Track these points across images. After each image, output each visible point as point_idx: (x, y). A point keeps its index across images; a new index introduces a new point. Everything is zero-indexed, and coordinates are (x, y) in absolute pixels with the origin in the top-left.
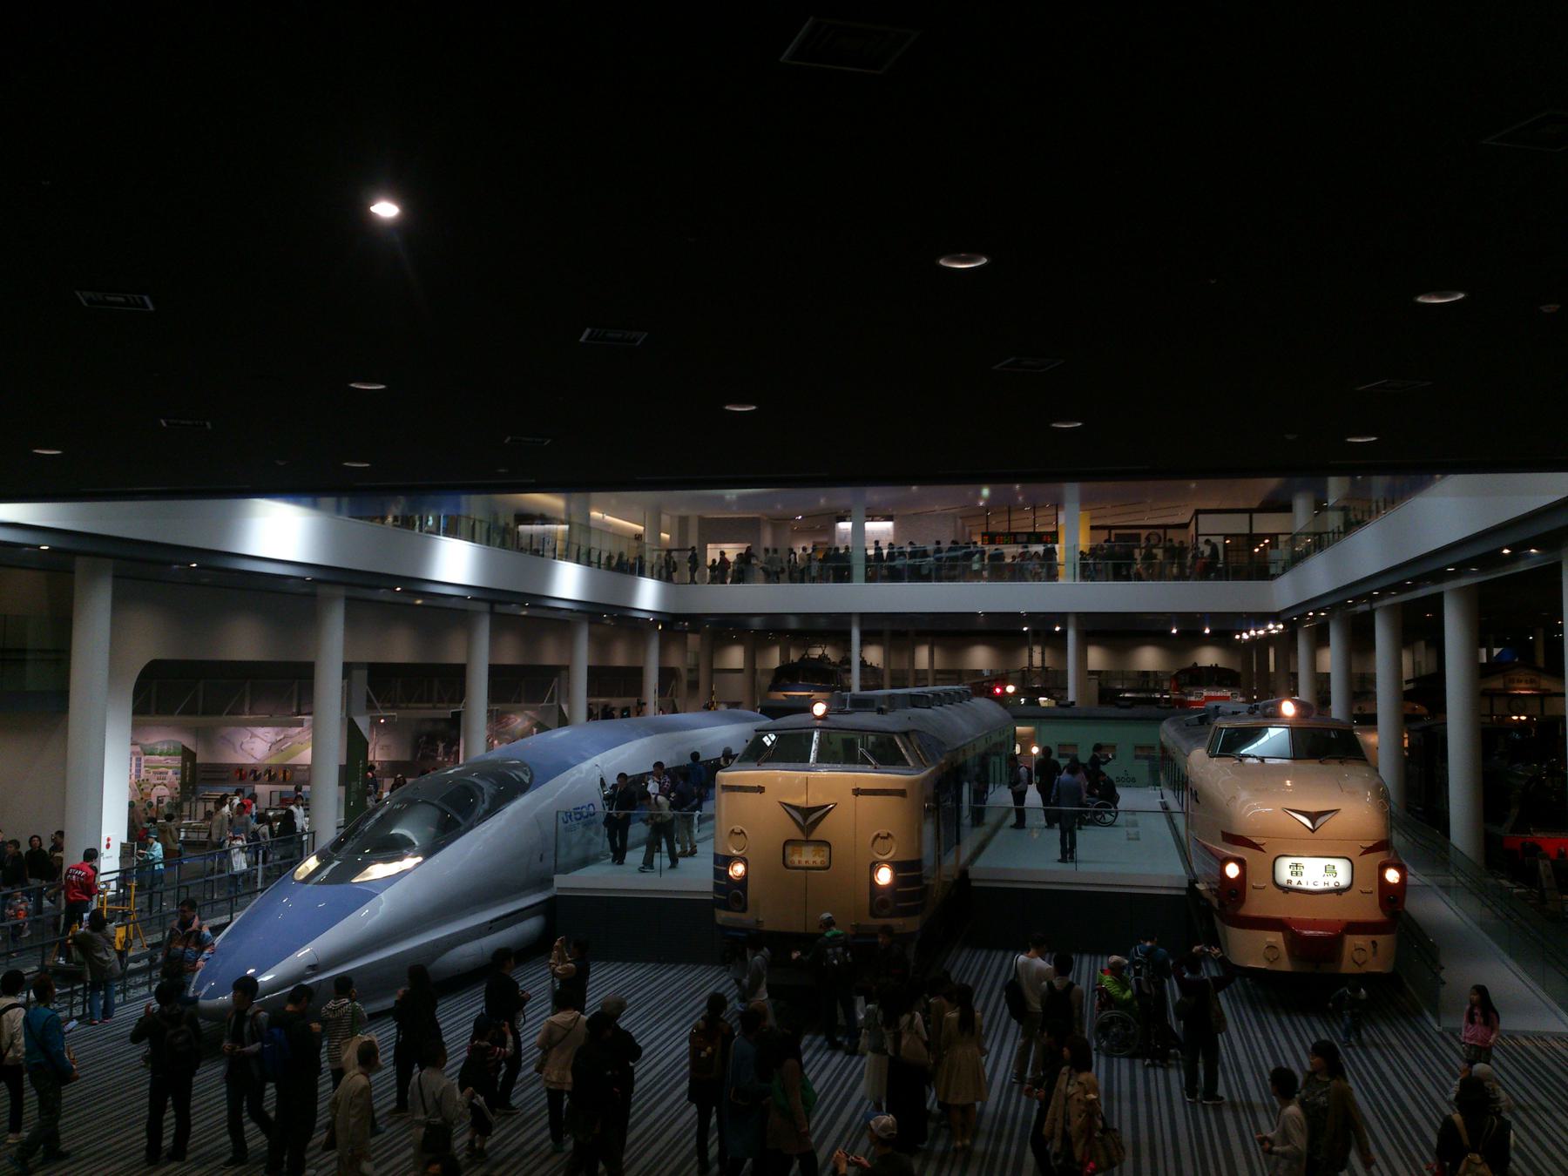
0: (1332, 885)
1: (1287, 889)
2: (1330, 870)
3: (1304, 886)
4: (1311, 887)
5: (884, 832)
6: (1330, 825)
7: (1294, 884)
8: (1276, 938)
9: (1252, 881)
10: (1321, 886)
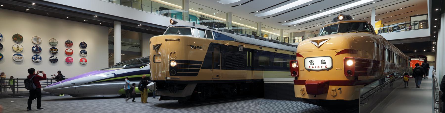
0: (324, 68)
1: (309, 70)
2: (323, 62)
3: (314, 69)
4: (317, 69)
5: (173, 51)
7: (311, 68)
9: (301, 68)
10: (320, 68)
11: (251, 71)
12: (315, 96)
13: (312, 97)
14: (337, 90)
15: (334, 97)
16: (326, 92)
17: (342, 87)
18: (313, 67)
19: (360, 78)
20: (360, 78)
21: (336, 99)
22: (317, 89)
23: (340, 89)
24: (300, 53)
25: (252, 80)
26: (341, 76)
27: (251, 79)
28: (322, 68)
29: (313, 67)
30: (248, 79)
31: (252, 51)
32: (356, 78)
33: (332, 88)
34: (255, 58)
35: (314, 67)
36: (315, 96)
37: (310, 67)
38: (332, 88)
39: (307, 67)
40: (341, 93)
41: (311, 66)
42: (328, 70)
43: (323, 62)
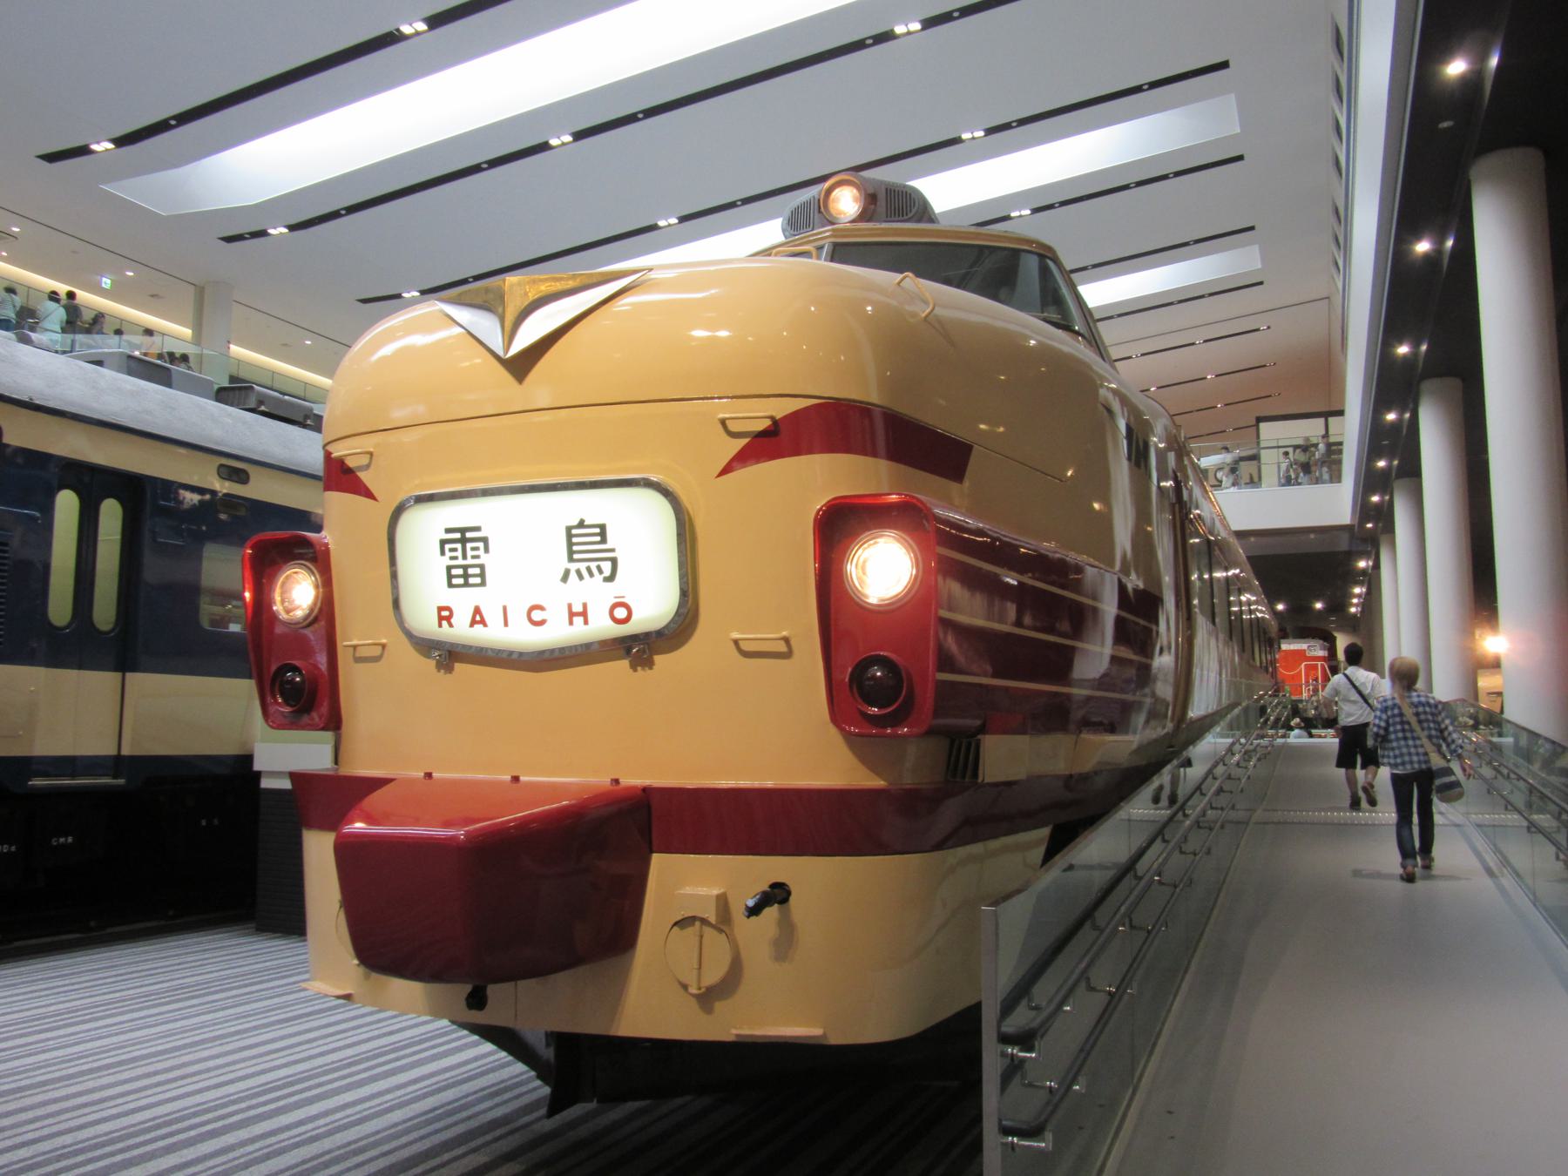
0: (601, 626)
3: (494, 635)
4: (522, 636)
7: (461, 631)
10: (557, 633)
11: (114, 677)
14: (738, 913)
15: (708, 998)
16: (618, 935)
18: (478, 618)
19: (1006, 757)
20: (1006, 757)
22: (510, 904)
23: (777, 894)
25: (118, 763)
26: (789, 738)
27: (103, 747)
28: (578, 633)
29: (478, 618)
30: (46, 745)
31: (135, 491)
32: (961, 756)
33: (681, 882)
34: (154, 569)
35: (492, 615)
37: (445, 614)
38: (681, 882)
40: (785, 942)
41: (462, 601)
42: (639, 648)
43: (588, 546)
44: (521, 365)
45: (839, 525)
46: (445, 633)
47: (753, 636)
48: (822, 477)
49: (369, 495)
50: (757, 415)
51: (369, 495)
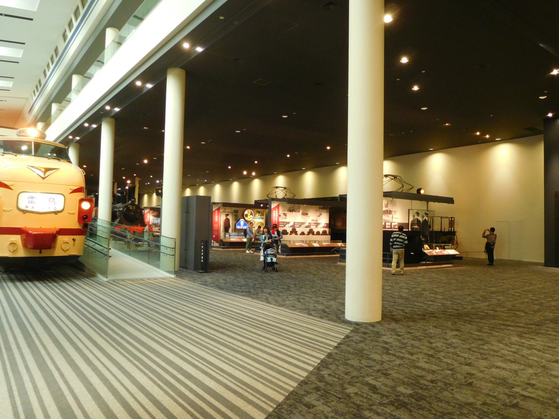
1: (24, 212)
6: (54, 176)
7: (30, 209)
8: (17, 239)
12: (41, 252)
13: (36, 254)
17: (77, 237)
18: (33, 208)
21: (66, 254)
24: (6, 183)
29: (33, 208)
33: (61, 239)
36: (41, 252)
38: (61, 239)
39: (22, 206)
42: (56, 213)
44: (43, 178)
45: (81, 201)
46: (27, 209)
47: (70, 212)
48: (81, 195)
49: (11, 189)
50: (75, 188)
51: (11, 189)
